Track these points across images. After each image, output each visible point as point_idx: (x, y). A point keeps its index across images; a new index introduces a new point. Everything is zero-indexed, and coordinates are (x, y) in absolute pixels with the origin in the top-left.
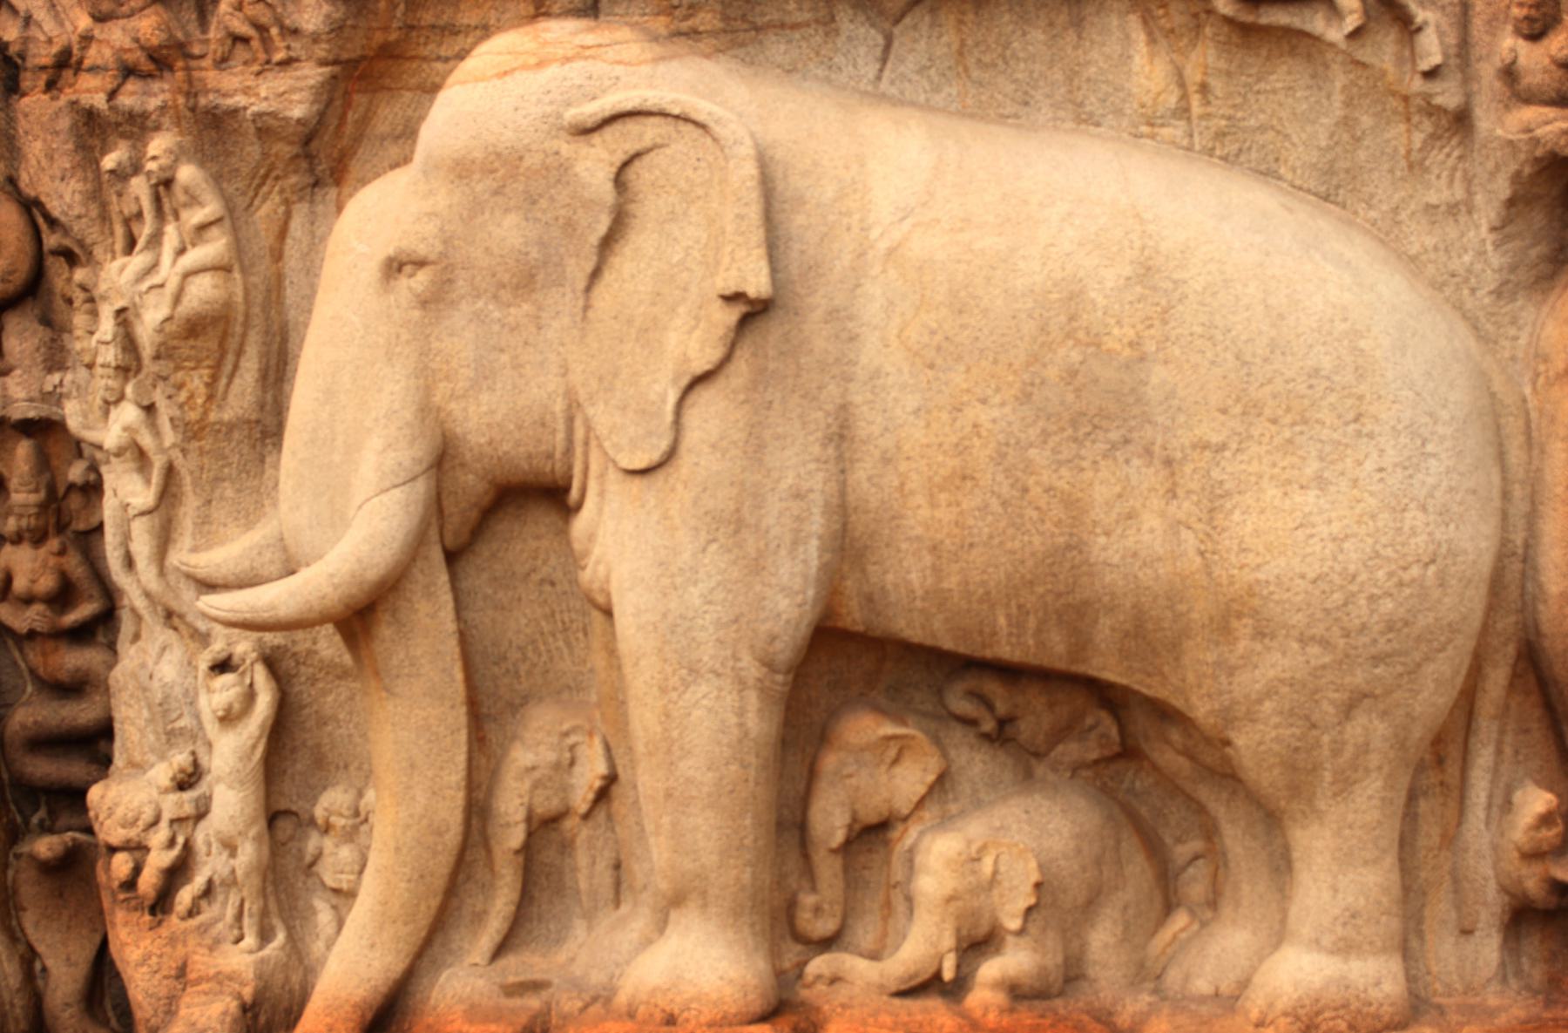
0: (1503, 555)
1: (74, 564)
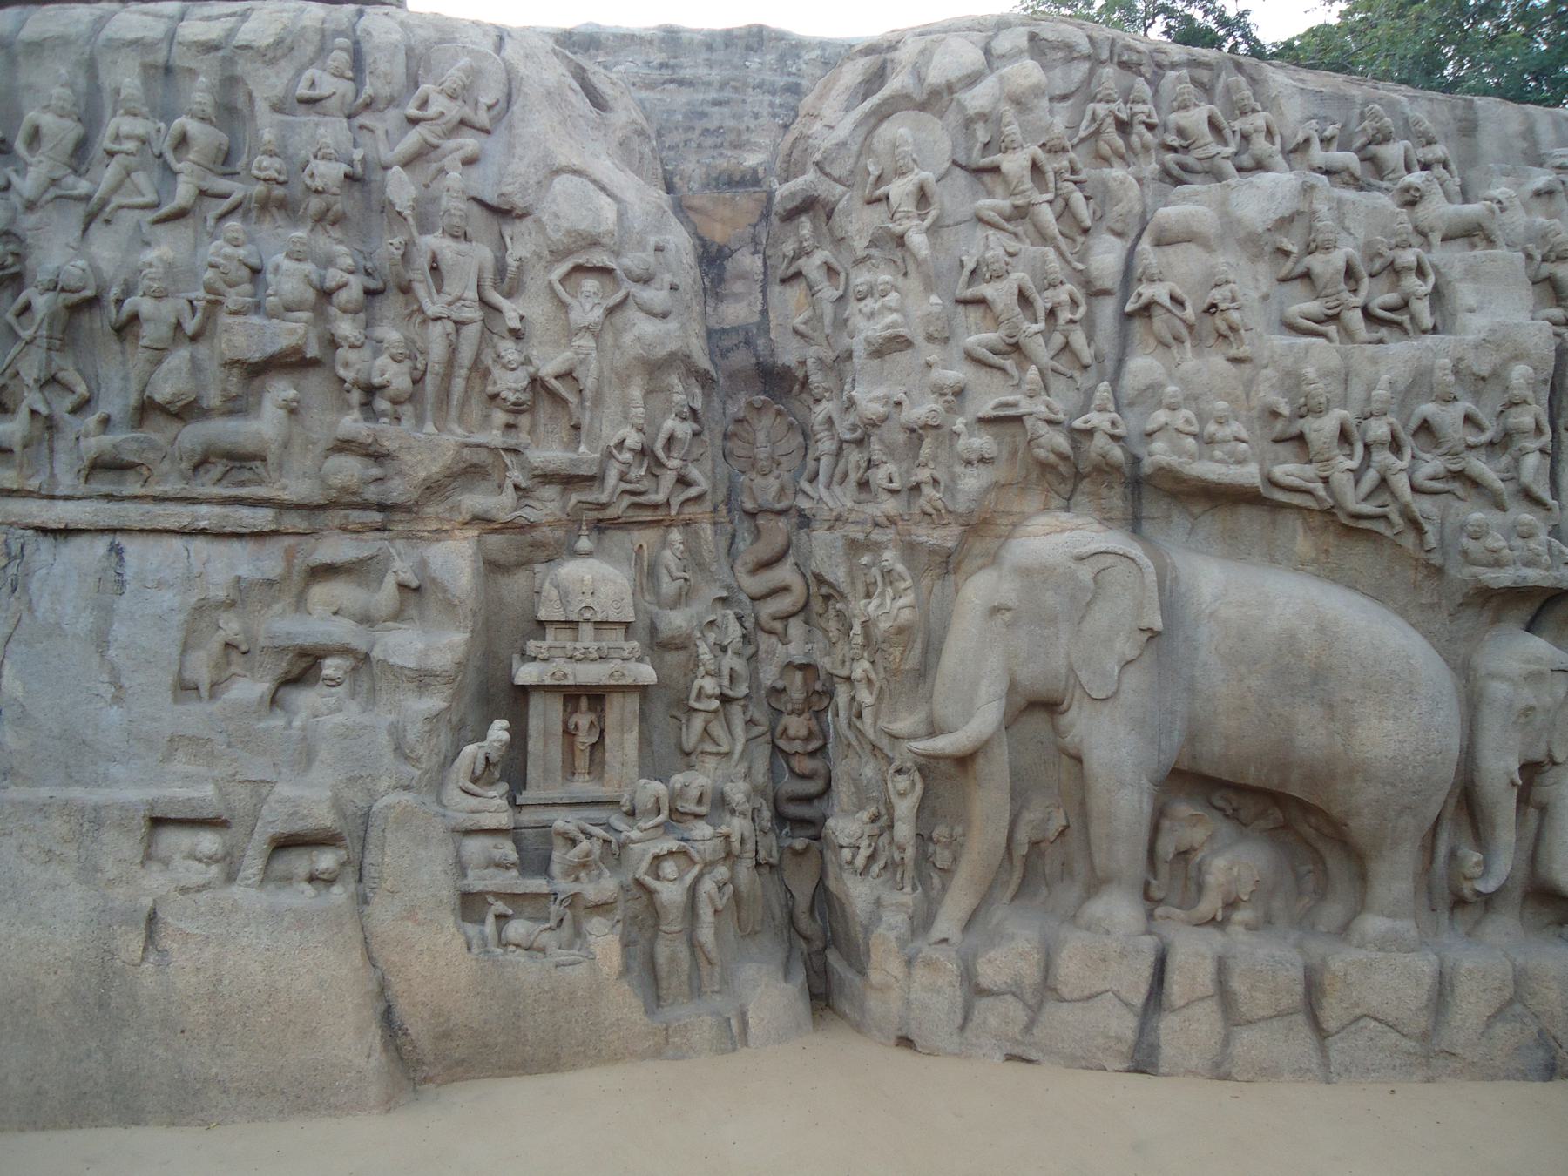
1: (814, 723)
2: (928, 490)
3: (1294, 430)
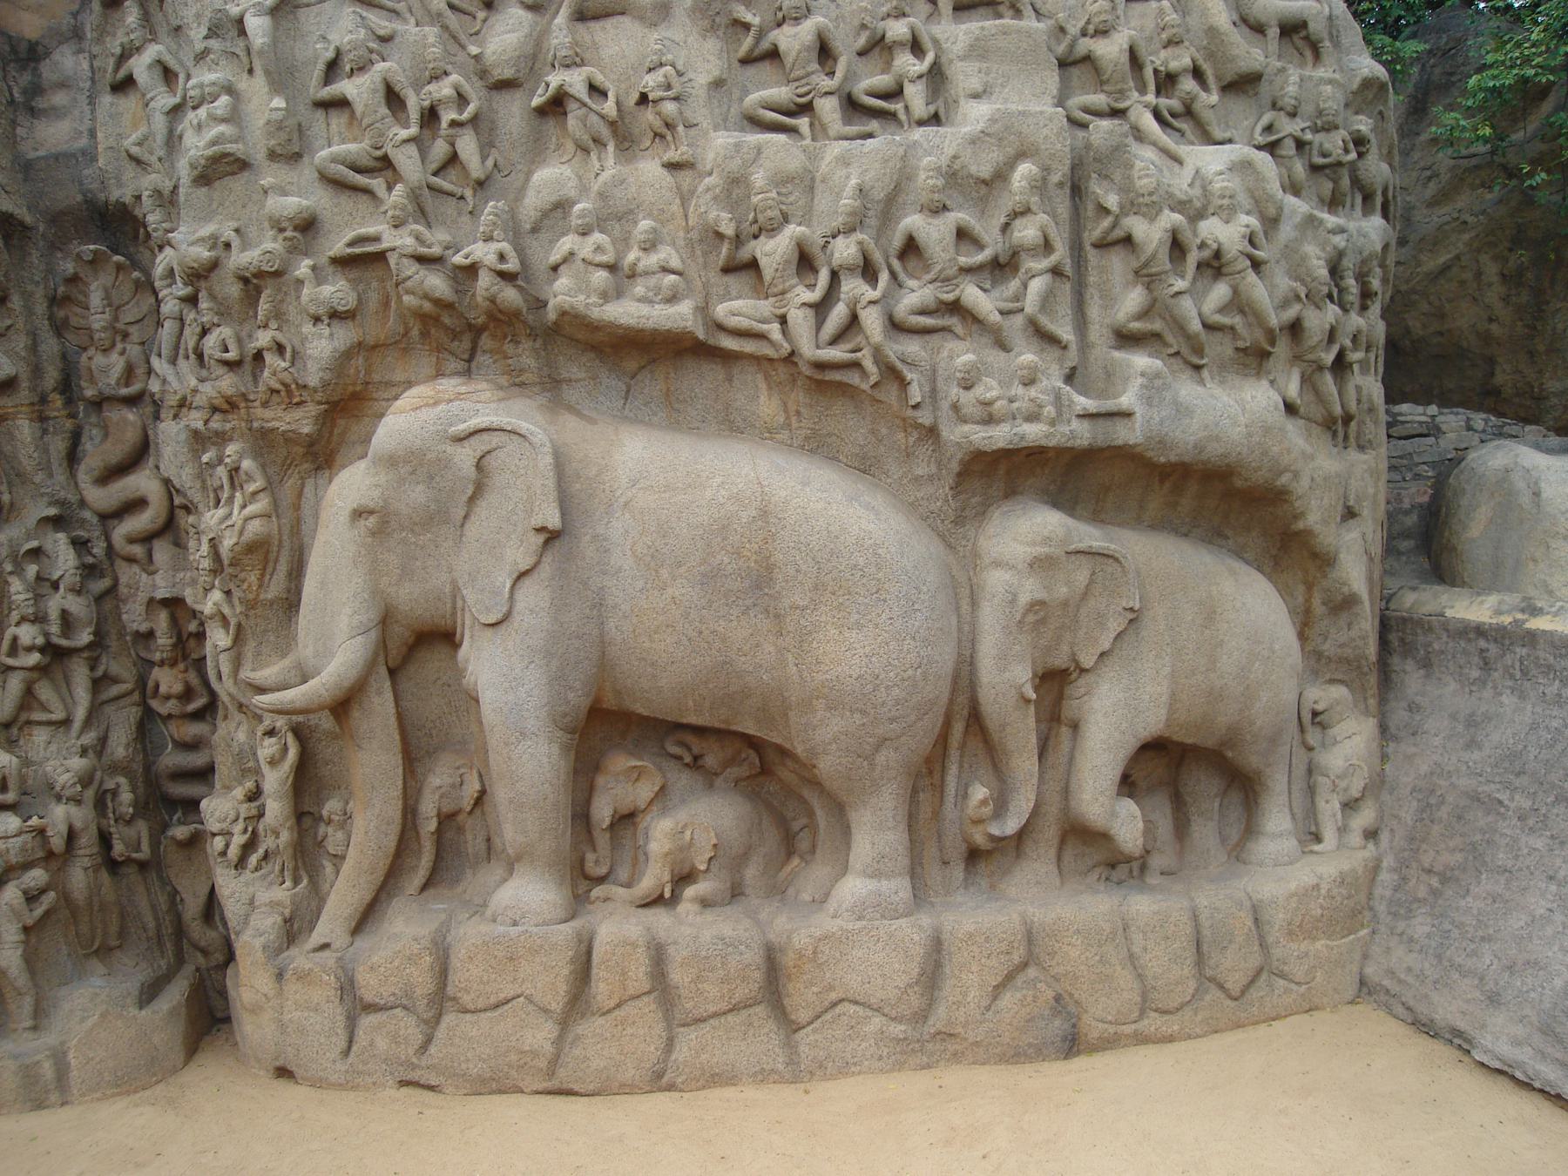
0: (959, 662)
1: (193, 677)
2: (269, 358)
3: (744, 254)
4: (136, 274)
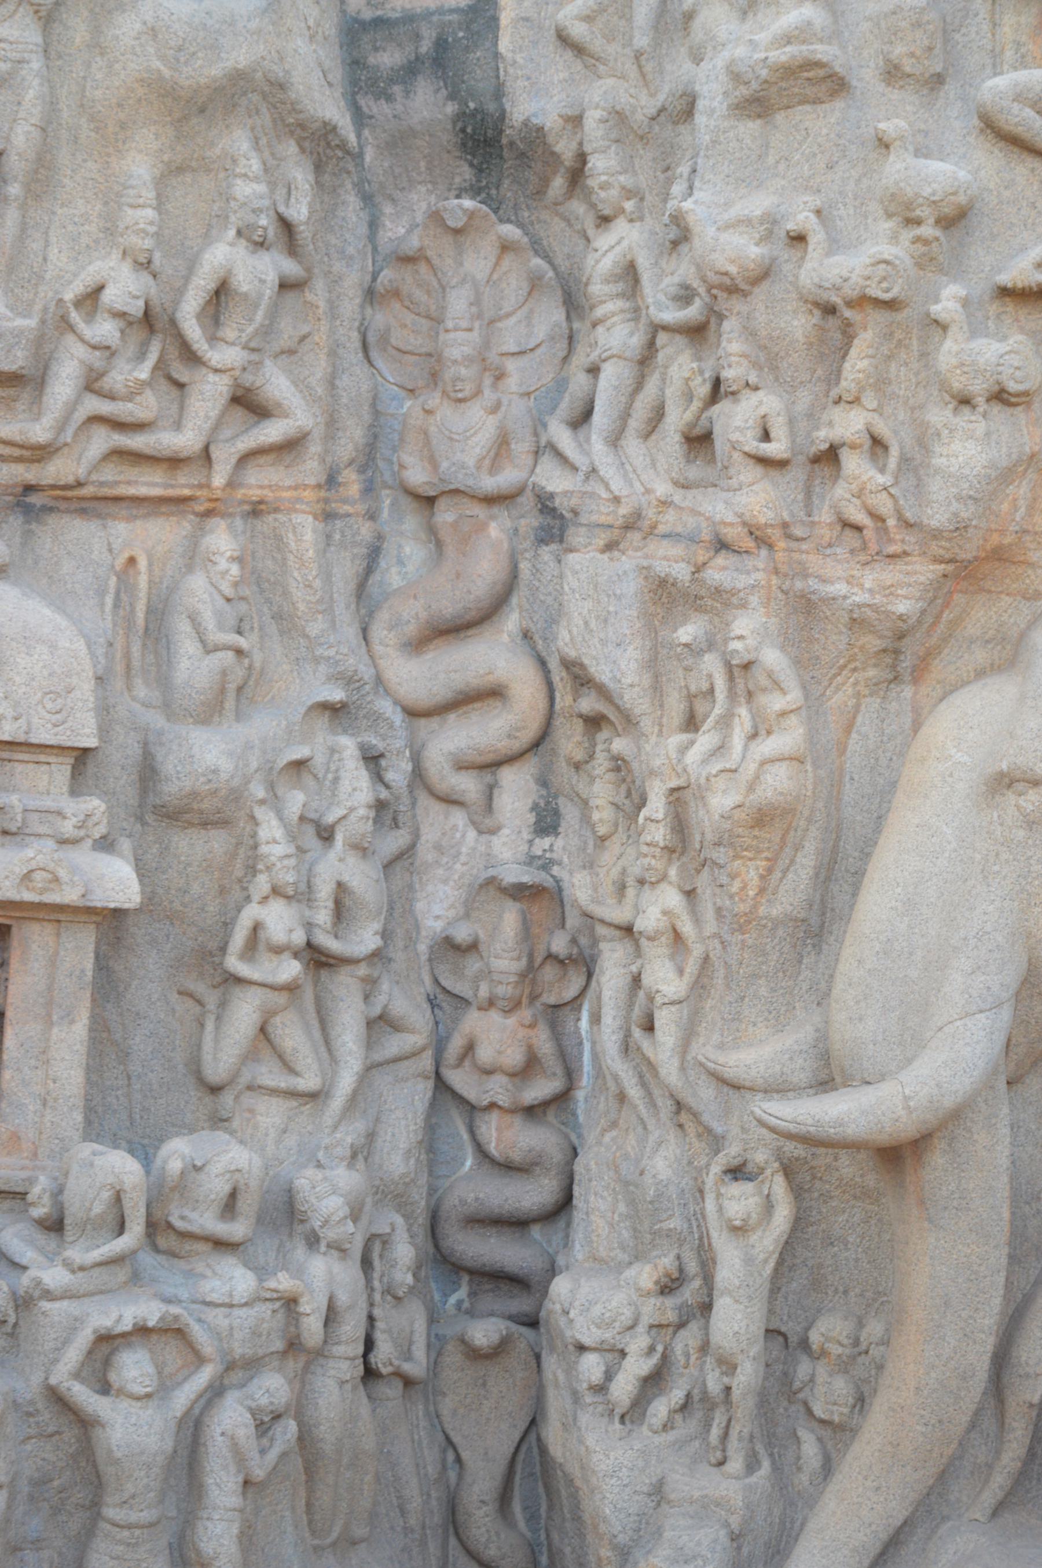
4: (537, 262)
